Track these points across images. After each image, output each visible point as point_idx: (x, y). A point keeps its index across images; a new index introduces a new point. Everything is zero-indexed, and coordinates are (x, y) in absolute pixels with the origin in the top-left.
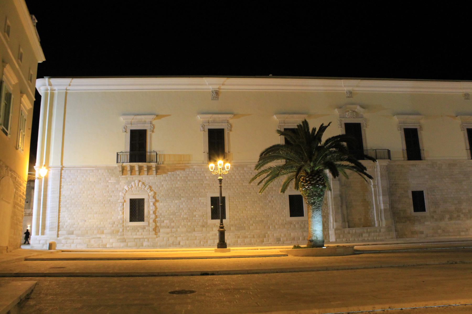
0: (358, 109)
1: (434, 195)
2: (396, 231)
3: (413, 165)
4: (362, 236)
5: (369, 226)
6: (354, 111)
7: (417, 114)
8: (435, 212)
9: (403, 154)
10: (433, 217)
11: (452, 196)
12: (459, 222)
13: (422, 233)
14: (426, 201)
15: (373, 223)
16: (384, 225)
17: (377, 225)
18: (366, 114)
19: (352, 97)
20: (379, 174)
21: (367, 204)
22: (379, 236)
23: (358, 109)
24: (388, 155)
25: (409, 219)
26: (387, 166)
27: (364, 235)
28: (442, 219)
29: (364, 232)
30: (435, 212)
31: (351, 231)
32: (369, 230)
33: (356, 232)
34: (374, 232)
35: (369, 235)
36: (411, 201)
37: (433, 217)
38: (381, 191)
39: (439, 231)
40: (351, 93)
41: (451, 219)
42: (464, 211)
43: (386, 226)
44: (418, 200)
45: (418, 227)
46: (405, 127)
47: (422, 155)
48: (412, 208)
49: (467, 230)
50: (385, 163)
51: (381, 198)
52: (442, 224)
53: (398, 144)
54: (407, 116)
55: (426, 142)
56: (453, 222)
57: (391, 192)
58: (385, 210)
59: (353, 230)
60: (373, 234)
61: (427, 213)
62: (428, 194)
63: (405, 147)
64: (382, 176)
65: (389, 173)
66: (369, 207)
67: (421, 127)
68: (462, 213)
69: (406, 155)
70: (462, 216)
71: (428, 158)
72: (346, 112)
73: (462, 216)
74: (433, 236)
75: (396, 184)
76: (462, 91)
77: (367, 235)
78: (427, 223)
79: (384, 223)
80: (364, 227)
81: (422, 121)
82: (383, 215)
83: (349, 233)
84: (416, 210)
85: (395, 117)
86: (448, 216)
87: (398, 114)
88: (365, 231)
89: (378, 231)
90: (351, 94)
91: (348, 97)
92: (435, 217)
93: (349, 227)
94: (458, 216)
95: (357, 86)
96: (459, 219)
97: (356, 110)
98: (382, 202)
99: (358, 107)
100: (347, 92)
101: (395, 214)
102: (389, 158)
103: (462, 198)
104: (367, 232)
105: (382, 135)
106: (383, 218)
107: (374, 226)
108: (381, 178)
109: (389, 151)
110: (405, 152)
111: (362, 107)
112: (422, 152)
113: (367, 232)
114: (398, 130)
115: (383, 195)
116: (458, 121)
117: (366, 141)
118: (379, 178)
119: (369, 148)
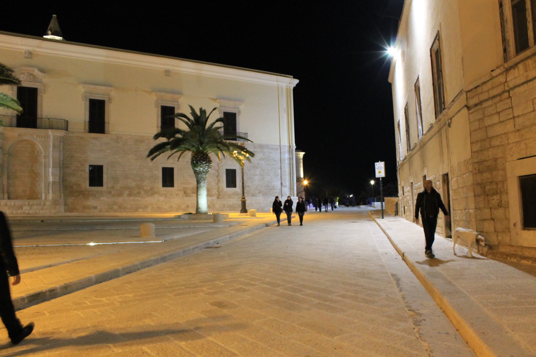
0: (36, 72)
1: (115, 171)
2: (65, 205)
3: (97, 139)
4: (22, 209)
5: (35, 199)
6: (31, 74)
7: (110, 86)
8: (113, 187)
9: (85, 126)
10: (110, 192)
11: (135, 172)
12: (139, 198)
13: (95, 208)
14: (105, 176)
15: (40, 196)
16: (51, 198)
17: (43, 198)
18: (46, 79)
19: (31, 58)
20: (51, 144)
21: (34, 176)
22: (43, 209)
23: (36, 72)
24: (65, 126)
25: (82, 194)
26: (63, 137)
27: (24, 208)
28: (120, 194)
29: (25, 205)
30: (113, 187)
31: (9, 203)
32: (31, 203)
33: (15, 205)
34: (36, 205)
35: (31, 208)
36: (87, 175)
37: (110, 192)
38: (51, 163)
39: (115, 207)
40: (30, 53)
41: (130, 195)
42: (145, 188)
43: (53, 199)
44: (96, 175)
45: (91, 202)
46: (92, 98)
47: (106, 129)
48: (88, 182)
49: (146, 206)
50: (60, 133)
51: (50, 170)
52: (120, 200)
53: (80, 115)
54: (94, 86)
55: (112, 115)
56: (131, 198)
57: (64, 166)
58: (54, 183)
59: (12, 202)
60: (35, 207)
61: (104, 188)
62: (108, 169)
63: (87, 119)
64: (54, 146)
65: (64, 144)
66: (37, 179)
67: (110, 99)
68: (144, 190)
69: (87, 127)
70: (143, 193)
71: (113, 133)
72: (22, 74)
73: (143, 193)
74: (107, 211)
75: (72, 157)
76: (163, 67)
77: (29, 208)
78: (102, 198)
79: (50, 196)
80: (28, 199)
81: (113, 93)
82: (51, 188)
83: (6, 205)
84: (92, 184)
85: (81, 87)
86: (127, 192)
87: (85, 83)
88: (27, 203)
89: (42, 204)
90: (30, 54)
91: (27, 58)
92: (113, 193)
93: (9, 198)
94: (139, 193)
95: (38, 47)
96: (139, 196)
97: (34, 74)
98: (50, 174)
99: (36, 70)
100: (25, 52)
101: (66, 187)
102: (67, 130)
103: (145, 175)
104: (29, 204)
105: (63, 103)
106: (51, 191)
107: (41, 198)
108: (53, 149)
109: (67, 122)
110: (87, 123)
111: (42, 70)
112: (106, 125)
113: (29, 204)
114: (83, 100)
115: (53, 167)
116: (154, 97)
117: (42, 107)
118: (51, 149)
119: (44, 117)
